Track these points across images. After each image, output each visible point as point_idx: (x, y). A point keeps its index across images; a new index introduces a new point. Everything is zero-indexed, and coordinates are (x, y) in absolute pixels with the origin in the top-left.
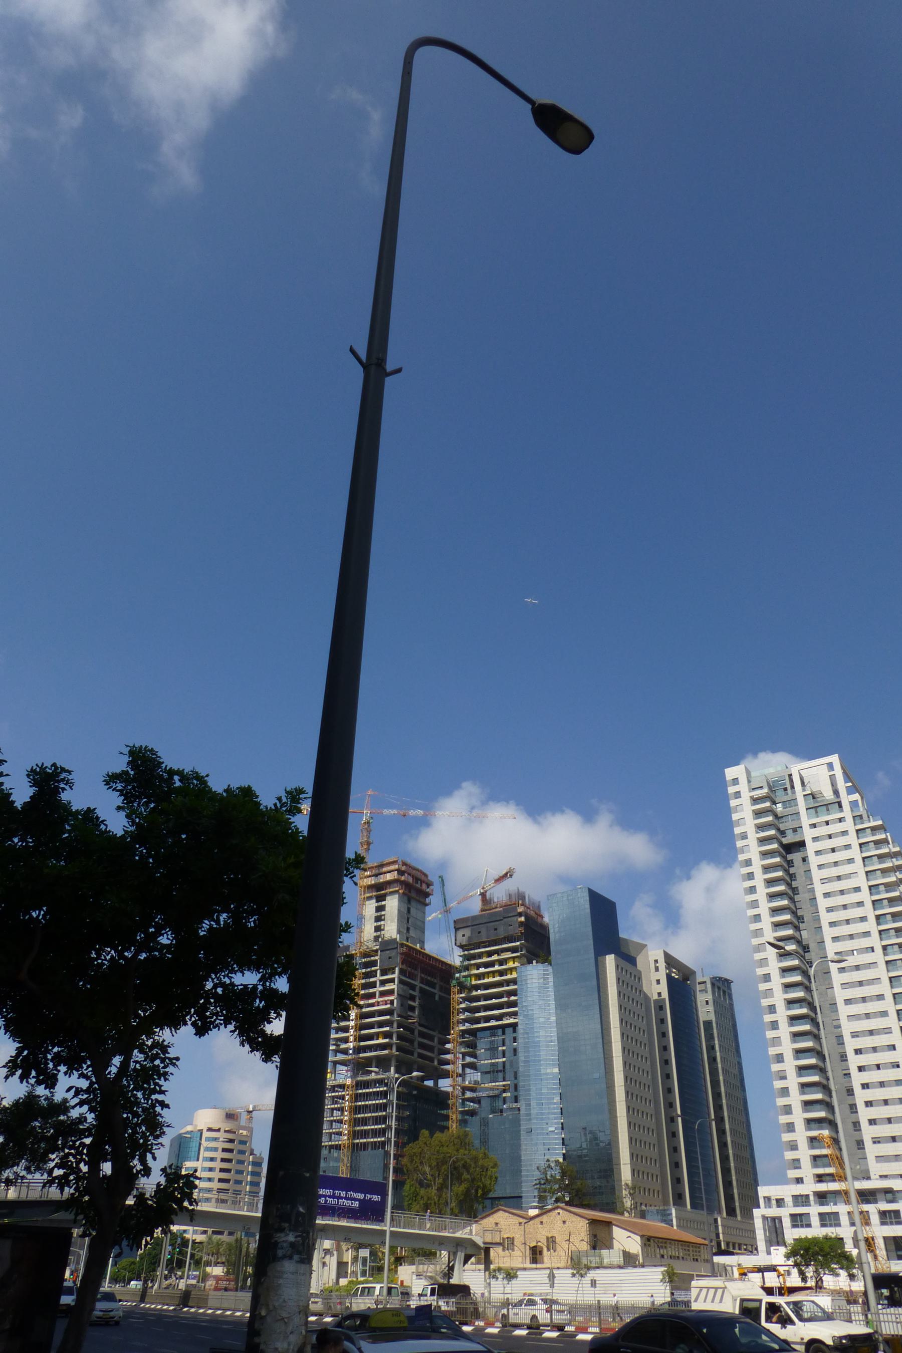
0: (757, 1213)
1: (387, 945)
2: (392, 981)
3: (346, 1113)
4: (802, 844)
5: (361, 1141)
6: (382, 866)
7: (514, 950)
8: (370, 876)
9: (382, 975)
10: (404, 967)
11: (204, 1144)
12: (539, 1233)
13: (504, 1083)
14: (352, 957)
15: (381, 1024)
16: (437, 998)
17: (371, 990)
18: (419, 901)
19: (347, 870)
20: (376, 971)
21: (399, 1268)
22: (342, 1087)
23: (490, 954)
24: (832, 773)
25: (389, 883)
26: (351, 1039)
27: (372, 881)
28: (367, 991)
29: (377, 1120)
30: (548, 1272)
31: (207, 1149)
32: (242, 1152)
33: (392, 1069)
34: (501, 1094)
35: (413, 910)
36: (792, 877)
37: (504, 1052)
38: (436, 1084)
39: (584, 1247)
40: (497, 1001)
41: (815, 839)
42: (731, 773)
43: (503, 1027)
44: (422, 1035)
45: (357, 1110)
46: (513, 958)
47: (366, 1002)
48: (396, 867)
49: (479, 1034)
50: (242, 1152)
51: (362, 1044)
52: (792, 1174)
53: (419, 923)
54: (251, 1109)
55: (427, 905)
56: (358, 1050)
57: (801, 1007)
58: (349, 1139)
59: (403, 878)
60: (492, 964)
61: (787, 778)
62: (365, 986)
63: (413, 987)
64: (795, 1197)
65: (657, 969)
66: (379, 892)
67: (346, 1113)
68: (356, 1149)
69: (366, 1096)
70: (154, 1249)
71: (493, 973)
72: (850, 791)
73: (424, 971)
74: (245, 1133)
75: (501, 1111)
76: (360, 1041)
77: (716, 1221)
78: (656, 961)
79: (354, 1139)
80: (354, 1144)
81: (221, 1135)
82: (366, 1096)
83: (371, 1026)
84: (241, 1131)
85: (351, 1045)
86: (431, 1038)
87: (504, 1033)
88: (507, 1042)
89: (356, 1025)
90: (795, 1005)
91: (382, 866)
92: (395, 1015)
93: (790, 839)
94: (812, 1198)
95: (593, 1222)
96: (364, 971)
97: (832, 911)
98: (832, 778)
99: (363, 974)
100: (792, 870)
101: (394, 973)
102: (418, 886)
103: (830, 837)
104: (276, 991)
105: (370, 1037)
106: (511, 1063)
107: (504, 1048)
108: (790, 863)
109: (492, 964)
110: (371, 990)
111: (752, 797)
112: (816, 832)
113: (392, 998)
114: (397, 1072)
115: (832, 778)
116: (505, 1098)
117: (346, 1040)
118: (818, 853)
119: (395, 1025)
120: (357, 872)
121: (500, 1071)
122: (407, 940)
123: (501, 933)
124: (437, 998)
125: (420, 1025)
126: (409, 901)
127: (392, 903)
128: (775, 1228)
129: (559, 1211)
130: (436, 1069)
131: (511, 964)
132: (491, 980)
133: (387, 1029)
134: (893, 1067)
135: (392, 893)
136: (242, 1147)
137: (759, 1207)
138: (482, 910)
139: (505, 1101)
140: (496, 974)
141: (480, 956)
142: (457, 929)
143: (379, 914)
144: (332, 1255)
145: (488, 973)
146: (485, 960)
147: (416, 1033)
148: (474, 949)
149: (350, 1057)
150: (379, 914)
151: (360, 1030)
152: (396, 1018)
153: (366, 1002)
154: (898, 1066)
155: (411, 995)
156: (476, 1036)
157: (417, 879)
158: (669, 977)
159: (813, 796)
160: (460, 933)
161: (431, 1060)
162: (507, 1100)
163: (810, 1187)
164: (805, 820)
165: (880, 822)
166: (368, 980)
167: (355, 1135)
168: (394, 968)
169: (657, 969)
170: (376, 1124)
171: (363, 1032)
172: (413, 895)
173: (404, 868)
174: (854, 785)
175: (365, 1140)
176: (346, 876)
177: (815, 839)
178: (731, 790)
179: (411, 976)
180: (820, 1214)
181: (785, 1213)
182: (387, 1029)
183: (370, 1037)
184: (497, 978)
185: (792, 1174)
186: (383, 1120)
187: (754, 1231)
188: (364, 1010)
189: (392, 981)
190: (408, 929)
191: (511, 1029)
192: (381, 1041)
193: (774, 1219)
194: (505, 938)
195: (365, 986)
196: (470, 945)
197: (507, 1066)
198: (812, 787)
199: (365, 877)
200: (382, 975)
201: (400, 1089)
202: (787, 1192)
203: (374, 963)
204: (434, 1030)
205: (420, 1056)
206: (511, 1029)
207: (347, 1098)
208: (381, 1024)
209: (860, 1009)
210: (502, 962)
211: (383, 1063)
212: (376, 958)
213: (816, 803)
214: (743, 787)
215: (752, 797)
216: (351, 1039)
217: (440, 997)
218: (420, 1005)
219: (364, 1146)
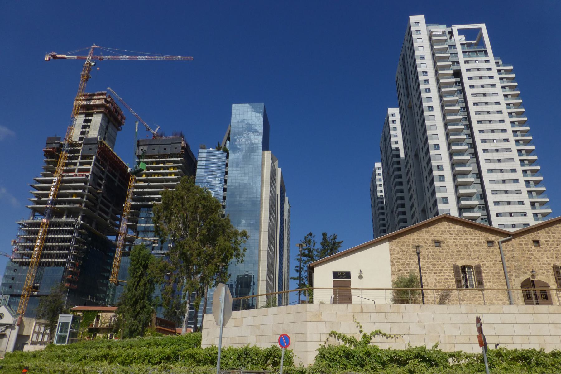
1: (89, 142)
2: (90, 163)
3: (39, 241)
5: (47, 260)
7: (175, 162)
8: (84, 100)
9: (82, 159)
10: (99, 157)
14: (61, 145)
16: (116, 184)
20: (78, 156)
21: (205, 315)
22: (38, 225)
23: (158, 163)
26: (53, 189)
29: (61, 248)
33: (80, 217)
34: (151, 245)
35: (110, 129)
40: (159, 190)
44: (102, 202)
45: (48, 240)
46: (174, 167)
48: (105, 97)
51: (59, 199)
55: (118, 130)
56: (54, 202)
58: (37, 258)
59: (108, 105)
60: (159, 169)
66: (89, 111)
68: (41, 265)
71: (159, 174)
80: (40, 262)
85: (51, 198)
86: (108, 207)
89: (57, 187)
91: (94, 95)
92: (88, 184)
96: (68, 155)
97: (479, 114)
99: (68, 157)
101: (92, 159)
102: (116, 115)
109: (159, 169)
113: (87, 174)
114: (82, 220)
119: (87, 191)
122: (104, 139)
123: (169, 151)
124: (116, 184)
125: (103, 196)
126: (108, 122)
127: (97, 120)
131: (172, 170)
132: (156, 177)
133: (81, 191)
134: (522, 215)
135: (98, 113)
141: (152, 163)
143: (85, 124)
145: (155, 174)
146: (154, 165)
147: (99, 201)
150: (84, 130)
151: (60, 189)
152: (88, 186)
153: (67, 174)
154: (525, 215)
155: (100, 176)
156: (139, 210)
157: (116, 111)
161: (106, 220)
162: (155, 248)
166: (70, 161)
167: (43, 256)
168: (92, 156)
171: (61, 191)
172: (112, 119)
173: (109, 100)
175: (50, 260)
179: (103, 165)
182: (81, 191)
186: (67, 248)
188: (64, 178)
195: (67, 165)
196: (146, 156)
199: (80, 100)
200: (82, 159)
201: (83, 231)
203: (78, 151)
207: (41, 231)
209: (500, 176)
210: (164, 168)
211: (72, 213)
212: (80, 148)
216: (52, 193)
218: (105, 184)
219: (49, 264)
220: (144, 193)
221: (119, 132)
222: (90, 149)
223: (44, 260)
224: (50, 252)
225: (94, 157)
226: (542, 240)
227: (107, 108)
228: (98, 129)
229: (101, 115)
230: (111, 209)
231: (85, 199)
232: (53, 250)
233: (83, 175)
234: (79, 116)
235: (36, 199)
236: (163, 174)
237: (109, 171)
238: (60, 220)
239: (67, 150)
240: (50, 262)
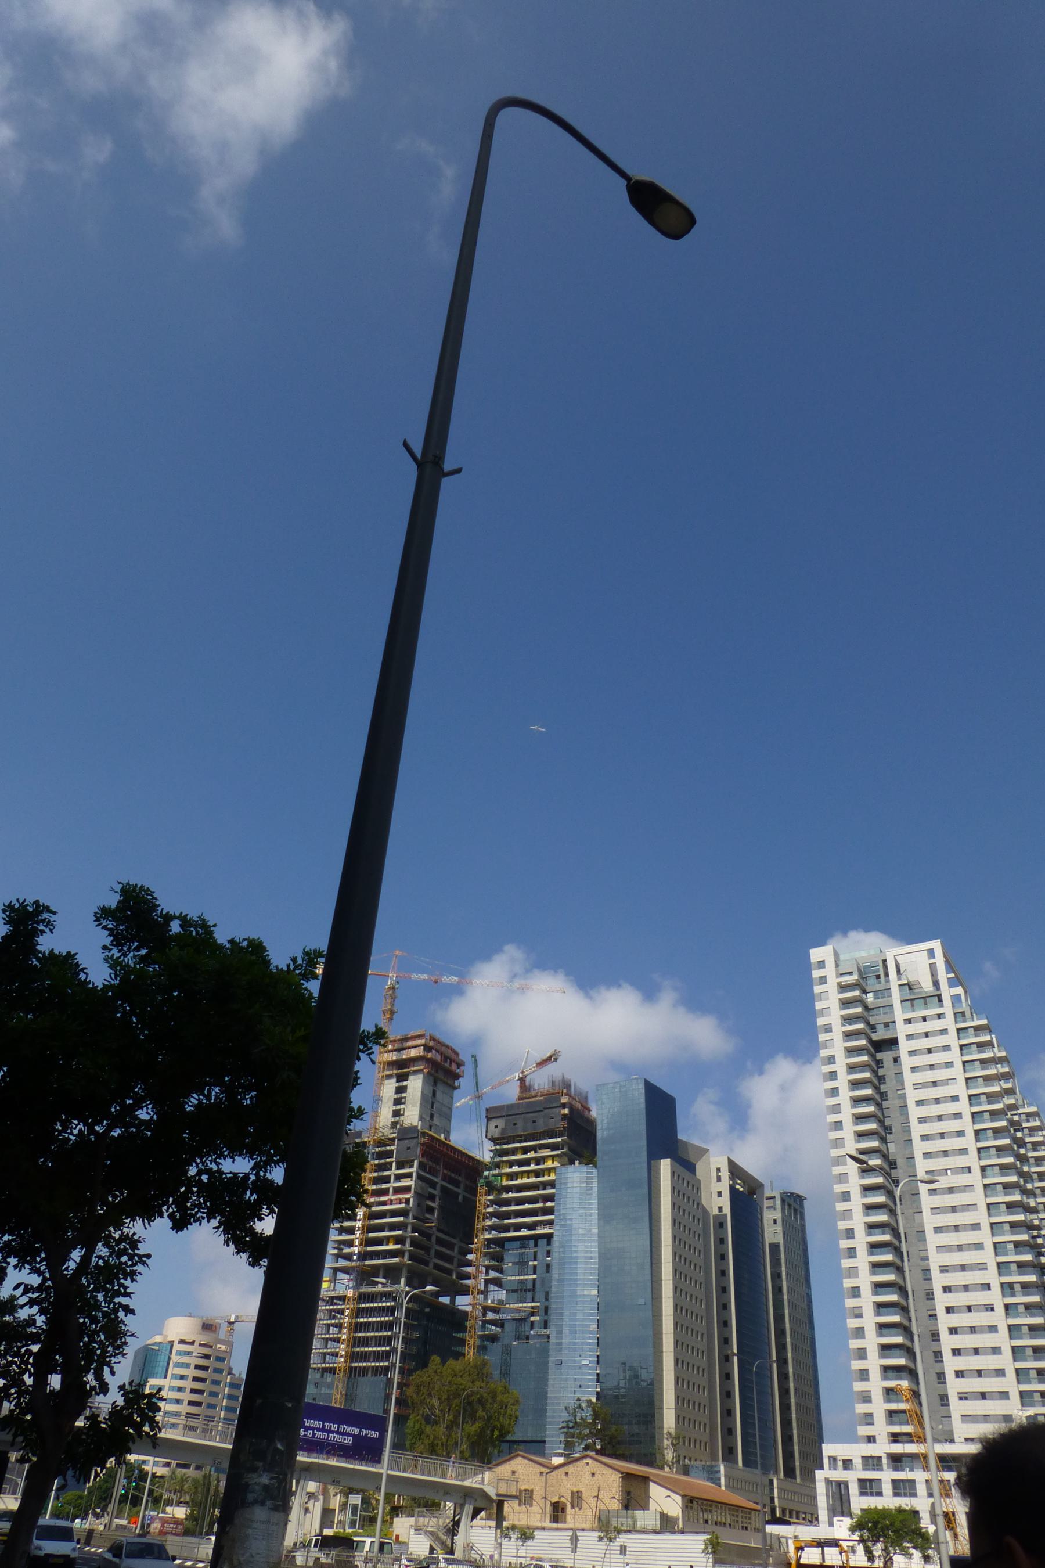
0: (819, 1475)
1: (406, 1134)
2: (409, 1176)
3: (345, 1331)
4: (893, 1042)
5: (360, 1364)
6: (406, 1039)
7: (553, 1147)
9: (398, 1168)
10: (424, 1160)
11: (175, 1358)
12: (563, 1486)
13: (533, 1304)
14: (364, 1144)
15: (393, 1227)
17: (384, 1186)
18: (447, 1084)
19: (365, 1045)
20: (391, 1163)
21: (395, 1520)
22: (342, 1299)
23: (526, 1150)
24: (932, 961)
25: (413, 1060)
26: (357, 1242)
27: (393, 1057)
28: (379, 1186)
29: (380, 1341)
30: (570, 1533)
31: (178, 1365)
32: (218, 1371)
33: (403, 1280)
35: (439, 1094)
36: (881, 1079)
37: (535, 1267)
38: (453, 1301)
39: (615, 1505)
40: (531, 1206)
41: (910, 1037)
42: (816, 954)
43: (536, 1238)
44: (440, 1242)
45: (357, 1327)
46: (553, 1157)
47: (377, 1199)
48: (423, 1041)
49: (507, 1245)
50: (218, 1371)
51: (369, 1249)
52: (864, 1431)
53: (444, 1109)
54: (233, 1320)
55: (455, 1088)
56: (364, 1256)
57: (884, 1233)
58: (346, 1362)
59: (430, 1055)
60: (527, 1162)
61: (881, 964)
62: (376, 1181)
63: (433, 1185)
64: (866, 1459)
65: (719, 1179)
66: (401, 1070)
67: (345, 1331)
68: (353, 1373)
69: (370, 1312)
70: (107, 1482)
72: (952, 983)
73: (446, 1166)
74: (223, 1347)
75: (528, 1338)
76: (367, 1245)
77: (771, 1482)
78: (719, 1170)
79: (352, 1362)
80: (351, 1368)
81: (195, 1349)
82: (370, 1312)
83: (381, 1228)
84: (219, 1346)
85: (356, 1250)
86: (451, 1246)
87: (536, 1245)
88: (540, 1256)
89: (363, 1226)
90: (877, 1231)
91: (406, 1039)
93: (880, 1035)
94: (884, 1461)
95: (627, 1477)
96: (377, 1162)
97: (925, 1122)
98: (933, 967)
99: (376, 1165)
100: (881, 1072)
101: (412, 1166)
102: (447, 1065)
103: (927, 1035)
104: (272, 1182)
105: (379, 1242)
106: (543, 1280)
107: (536, 1263)
108: (879, 1063)
109: (527, 1162)
110: (384, 1186)
111: (839, 984)
112: (911, 1029)
113: (407, 1196)
114: (407, 1284)
115: (933, 967)
116: (532, 1322)
117: (350, 1244)
118: (912, 1053)
119: (409, 1229)
120: (376, 1048)
121: (530, 1290)
123: (541, 1126)
124: (460, 1198)
125: (439, 1230)
126: (435, 1083)
127: (415, 1084)
128: (839, 1494)
129: (588, 1460)
130: (454, 1283)
131: (549, 1164)
132: (525, 1181)
133: (400, 1232)
134: (987, 1310)
135: (416, 1072)
136: (219, 1365)
137: (822, 1468)
138: (520, 1098)
139: (532, 1325)
140: (532, 1175)
141: (514, 1151)
142: (489, 1119)
144: (316, 1499)
146: (520, 1157)
148: (507, 1143)
149: (354, 1264)
151: (368, 1232)
152: (410, 1220)
153: (377, 1199)
154: (992, 1309)
156: (503, 1247)
157: (446, 1058)
158: (732, 1189)
159: (910, 986)
160: (493, 1124)
161: (449, 1272)
162: (536, 1325)
163: (883, 1448)
164: (899, 1014)
165: (985, 1022)
166: (381, 1174)
167: (353, 1357)
168: (412, 1161)
169: (719, 1179)
170: (380, 1346)
171: (371, 1235)
172: (441, 1075)
173: (431, 1044)
174: (957, 976)
175: (365, 1364)
176: (363, 1052)
177: (910, 1037)
178: (816, 974)
179: (433, 1172)
180: (893, 1481)
181: (852, 1477)
182: (400, 1232)
183: (379, 1242)
184: (533, 1180)
185: (864, 1431)
186: (388, 1341)
187: (815, 1497)
188: (374, 1209)
189: (409, 1176)
190: (432, 1116)
191: (545, 1241)
192: (391, 1247)
193: (839, 1484)
194: (544, 1132)
195: (376, 1181)
196: (504, 1138)
197: (538, 1283)
198: (910, 976)
200: (398, 1168)
201: (410, 1305)
202: (856, 1451)
203: (389, 1154)
204: (454, 1238)
205: (437, 1267)
206: (545, 1241)
207: (347, 1312)
208: (393, 1227)
210: (539, 1161)
211: (392, 1273)
212: (392, 1148)
213: (913, 995)
214: (830, 971)
215: (839, 984)
216: (357, 1242)
217: (464, 1197)
218: (440, 1206)
219: (364, 1371)
220: (507, 1215)
221: (455, 1092)
222: (408, 1148)
223: (356, 1365)
224: (362, 1349)
225: (416, 1163)
226: (570, 1472)
227: (429, 1061)
228: (418, 1105)
229: (421, 1076)
230: (456, 1250)
231: (407, 1245)
232: (367, 1346)
233: (400, 1202)
234: (386, 1082)
235: (336, 1251)
236: (537, 1174)
237: (445, 1178)
238: (374, 1290)
239: (373, 1154)
240: (364, 1367)
